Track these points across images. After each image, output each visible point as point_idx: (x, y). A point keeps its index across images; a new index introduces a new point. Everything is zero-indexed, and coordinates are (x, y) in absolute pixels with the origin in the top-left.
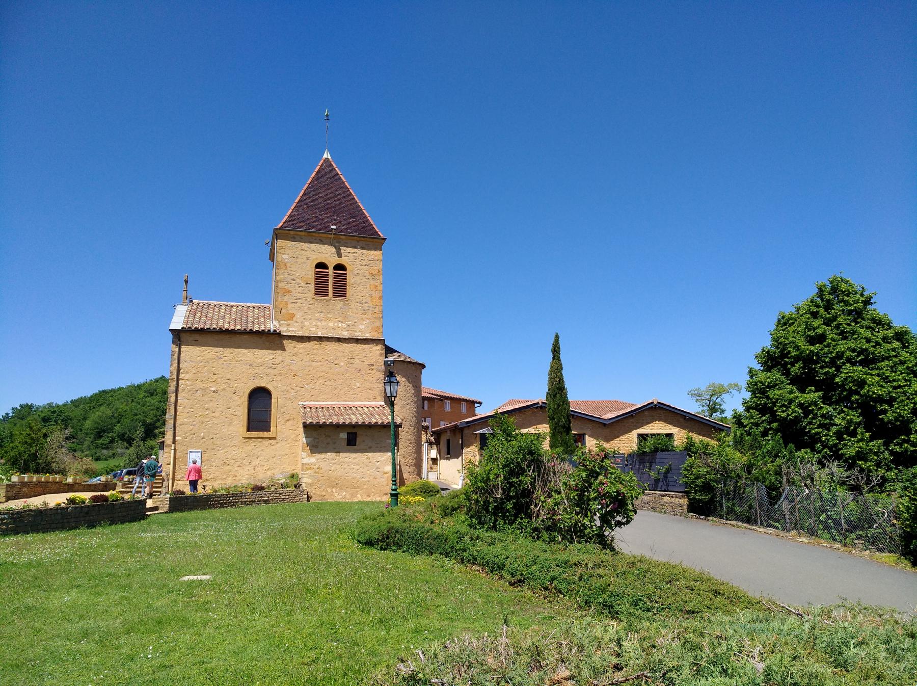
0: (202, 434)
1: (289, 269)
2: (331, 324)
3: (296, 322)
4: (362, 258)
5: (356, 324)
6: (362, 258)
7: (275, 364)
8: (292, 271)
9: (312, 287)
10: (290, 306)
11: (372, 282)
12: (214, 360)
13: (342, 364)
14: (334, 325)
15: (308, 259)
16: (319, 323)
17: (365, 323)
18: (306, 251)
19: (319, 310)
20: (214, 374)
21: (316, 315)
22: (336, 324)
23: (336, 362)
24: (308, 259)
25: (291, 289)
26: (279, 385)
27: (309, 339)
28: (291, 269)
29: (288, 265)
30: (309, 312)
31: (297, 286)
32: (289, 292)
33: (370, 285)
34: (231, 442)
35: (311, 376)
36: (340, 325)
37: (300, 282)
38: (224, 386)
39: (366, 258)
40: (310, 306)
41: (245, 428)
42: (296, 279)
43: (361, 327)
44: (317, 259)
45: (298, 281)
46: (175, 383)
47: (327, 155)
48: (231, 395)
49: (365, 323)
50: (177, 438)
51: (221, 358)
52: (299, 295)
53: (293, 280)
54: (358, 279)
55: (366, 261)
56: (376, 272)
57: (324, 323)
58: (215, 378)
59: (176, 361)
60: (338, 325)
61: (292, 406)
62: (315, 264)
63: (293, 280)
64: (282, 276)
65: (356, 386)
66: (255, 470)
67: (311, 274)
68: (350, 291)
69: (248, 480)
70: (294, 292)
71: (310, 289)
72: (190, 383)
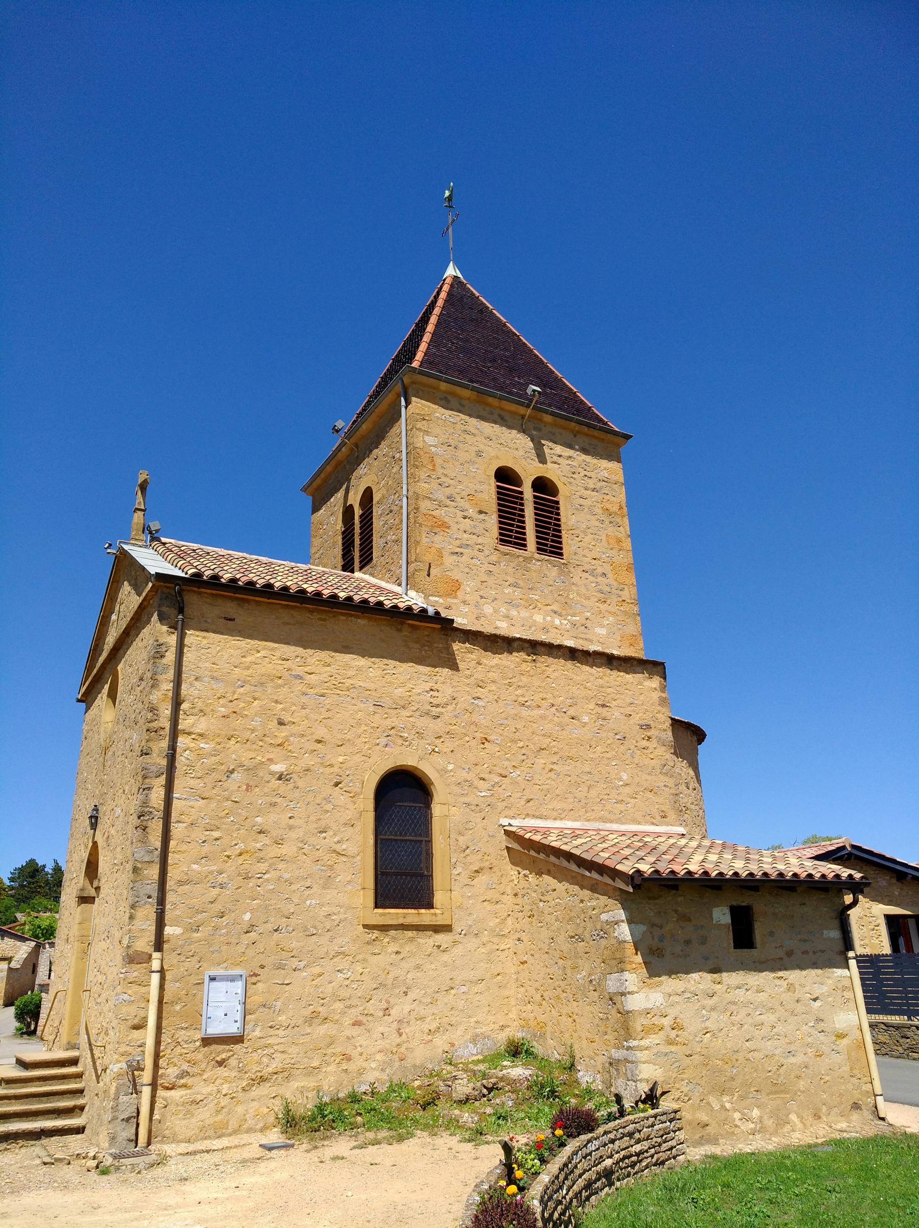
0: (247, 916)
1: (440, 471)
2: (539, 618)
3: (464, 602)
4: (586, 473)
5: (588, 624)
6: (586, 473)
7: (437, 706)
8: (446, 475)
9: (492, 521)
10: (449, 560)
11: (611, 530)
12: (280, 681)
13: (586, 719)
14: (544, 619)
16: (514, 613)
19: (511, 580)
20: (281, 723)
22: (549, 618)
23: (572, 712)
24: (479, 454)
26: (451, 767)
29: (438, 461)
30: (491, 581)
31: (460, 514)
32: (444, 526)
35: (520, 744)
36: (557, 622)
37: (466, 505)
38: (308, 760)
40: (492, 568)
42: (458, 499)
43: (603, 631)
45: (462, 503)
46: (165, 744)
47: (451, 271)
48: (328, 790)
50: (168, 930)
52: (465, 536)
56: (615, 508)
57: (524, 613)
58: (283, 733)
59: (171, 674)
64: (426, 485)
65: (620, 779)
67: (489, 491)
68: (568, 544)
70: (454, 527)
71: (488, 525)
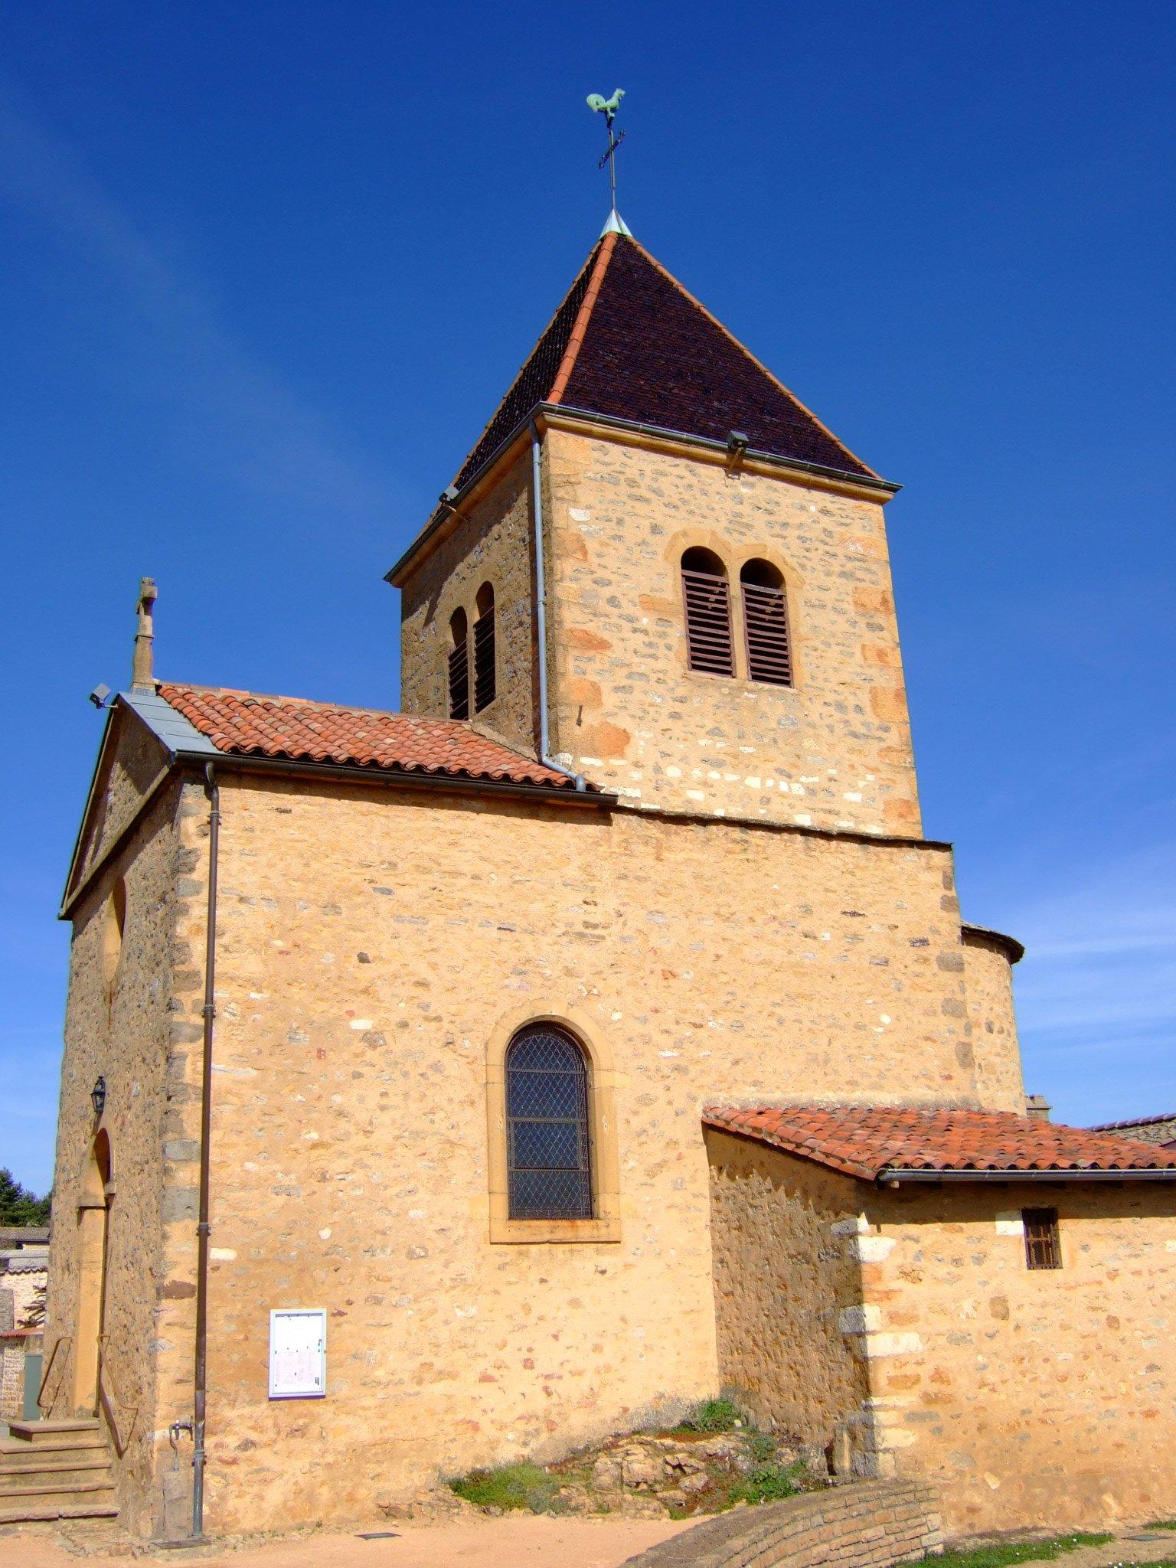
0: (326, 1233)
1: (593, 559)
2: (753, 782)
3: (637, 765)
4: (827, 548)
5: (833, 786)
6: (827, 548)
7: (595, 926)
8: (605, 567)
9: (677, 631)
10: (610, 700)
11: (871, 638)
12: (359, 899)
13: (827, 936)
14: (763, 783)
15: (655, 529)
16: (714, 775)
17: (861, 784)
18: (647, 501)
19: (710, 725)
20: (363, 959)
21: (702, 742)
22: (770, 783)
23: (805, 925)
24: (655, 529)
25: (606, 635)
26: (617, 1016)
27: (704, 821)
28: (603, 561)
29: (592, 546)
30: (677, 727)
31: (627, 626)
32: (603, 645)
33: (863, 647)
34: (446, 1265)
35: (723, 978)
36: (783, 786)
37: (637, 611)
38: (403, 1010)
39: (839, 551)
40: (678, 707)
41: (501, 1203)
42: (624, 603)
43: (855, 797)
44: (685, 534)
45: (628, 609)
46: (200, 994)
47: (615, 225)
48: (437, 1054)
49: (861, 784)
50: (215, 1254)
51: (389, 892)
52: (636, 660)
53: (613, 601)
54: (822, 619)
55: (842, 559)
56: (876, 600)
57: (731, 777)
58: (368, 972)
59: (204, 895)
60: (776, 786)
61: (670, 1103)
62: (688, 546)
63: (613, 601)
64: (574, 585)
65: (880, 1024)
66: (549, 1394)
67: (671, 585)
68: (802, 658)
69: (525, 1444)
70: (618, 646)
71: (668, 641)
72: (266, 995)
